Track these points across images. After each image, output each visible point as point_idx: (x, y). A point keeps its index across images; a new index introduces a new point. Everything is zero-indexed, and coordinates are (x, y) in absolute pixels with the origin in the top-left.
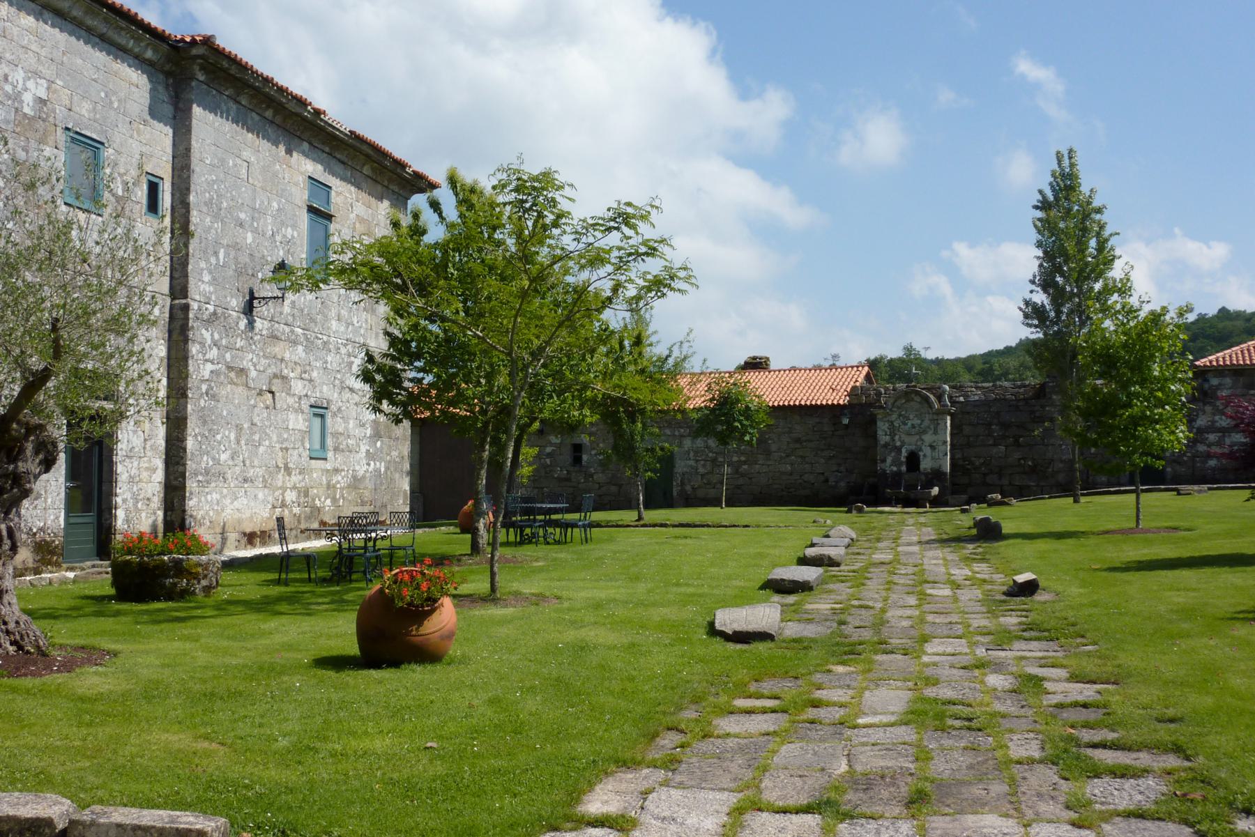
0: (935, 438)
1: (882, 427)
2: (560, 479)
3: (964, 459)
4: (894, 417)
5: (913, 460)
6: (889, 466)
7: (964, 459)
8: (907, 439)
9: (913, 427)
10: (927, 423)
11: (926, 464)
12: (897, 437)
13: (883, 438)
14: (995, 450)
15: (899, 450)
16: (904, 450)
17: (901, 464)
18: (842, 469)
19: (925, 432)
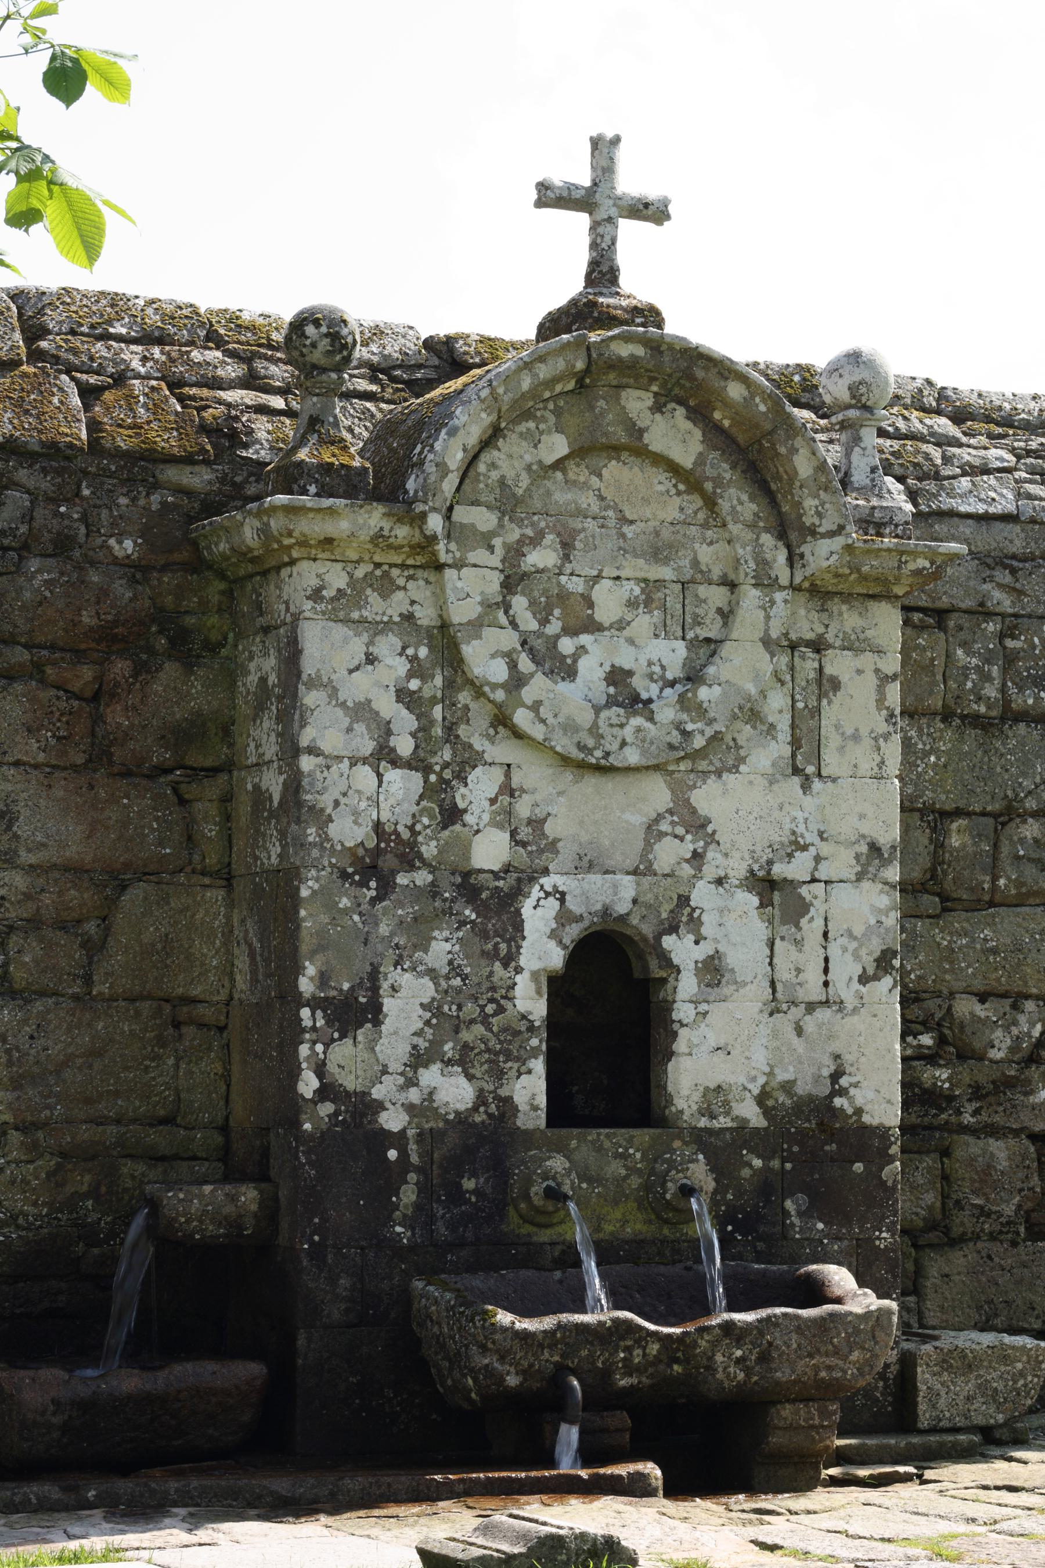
0: (801, 809)
1: (350, 674)
4: (470, 587)
6: (408, 1057)
8: (571, 811)
9: (623, 692)
10: (743, 666)
11: (721, 1056)
12: (478, 791)
13: (361, 798)
15: (491, 906)
16: (537, 916)
17: (496, 1060)
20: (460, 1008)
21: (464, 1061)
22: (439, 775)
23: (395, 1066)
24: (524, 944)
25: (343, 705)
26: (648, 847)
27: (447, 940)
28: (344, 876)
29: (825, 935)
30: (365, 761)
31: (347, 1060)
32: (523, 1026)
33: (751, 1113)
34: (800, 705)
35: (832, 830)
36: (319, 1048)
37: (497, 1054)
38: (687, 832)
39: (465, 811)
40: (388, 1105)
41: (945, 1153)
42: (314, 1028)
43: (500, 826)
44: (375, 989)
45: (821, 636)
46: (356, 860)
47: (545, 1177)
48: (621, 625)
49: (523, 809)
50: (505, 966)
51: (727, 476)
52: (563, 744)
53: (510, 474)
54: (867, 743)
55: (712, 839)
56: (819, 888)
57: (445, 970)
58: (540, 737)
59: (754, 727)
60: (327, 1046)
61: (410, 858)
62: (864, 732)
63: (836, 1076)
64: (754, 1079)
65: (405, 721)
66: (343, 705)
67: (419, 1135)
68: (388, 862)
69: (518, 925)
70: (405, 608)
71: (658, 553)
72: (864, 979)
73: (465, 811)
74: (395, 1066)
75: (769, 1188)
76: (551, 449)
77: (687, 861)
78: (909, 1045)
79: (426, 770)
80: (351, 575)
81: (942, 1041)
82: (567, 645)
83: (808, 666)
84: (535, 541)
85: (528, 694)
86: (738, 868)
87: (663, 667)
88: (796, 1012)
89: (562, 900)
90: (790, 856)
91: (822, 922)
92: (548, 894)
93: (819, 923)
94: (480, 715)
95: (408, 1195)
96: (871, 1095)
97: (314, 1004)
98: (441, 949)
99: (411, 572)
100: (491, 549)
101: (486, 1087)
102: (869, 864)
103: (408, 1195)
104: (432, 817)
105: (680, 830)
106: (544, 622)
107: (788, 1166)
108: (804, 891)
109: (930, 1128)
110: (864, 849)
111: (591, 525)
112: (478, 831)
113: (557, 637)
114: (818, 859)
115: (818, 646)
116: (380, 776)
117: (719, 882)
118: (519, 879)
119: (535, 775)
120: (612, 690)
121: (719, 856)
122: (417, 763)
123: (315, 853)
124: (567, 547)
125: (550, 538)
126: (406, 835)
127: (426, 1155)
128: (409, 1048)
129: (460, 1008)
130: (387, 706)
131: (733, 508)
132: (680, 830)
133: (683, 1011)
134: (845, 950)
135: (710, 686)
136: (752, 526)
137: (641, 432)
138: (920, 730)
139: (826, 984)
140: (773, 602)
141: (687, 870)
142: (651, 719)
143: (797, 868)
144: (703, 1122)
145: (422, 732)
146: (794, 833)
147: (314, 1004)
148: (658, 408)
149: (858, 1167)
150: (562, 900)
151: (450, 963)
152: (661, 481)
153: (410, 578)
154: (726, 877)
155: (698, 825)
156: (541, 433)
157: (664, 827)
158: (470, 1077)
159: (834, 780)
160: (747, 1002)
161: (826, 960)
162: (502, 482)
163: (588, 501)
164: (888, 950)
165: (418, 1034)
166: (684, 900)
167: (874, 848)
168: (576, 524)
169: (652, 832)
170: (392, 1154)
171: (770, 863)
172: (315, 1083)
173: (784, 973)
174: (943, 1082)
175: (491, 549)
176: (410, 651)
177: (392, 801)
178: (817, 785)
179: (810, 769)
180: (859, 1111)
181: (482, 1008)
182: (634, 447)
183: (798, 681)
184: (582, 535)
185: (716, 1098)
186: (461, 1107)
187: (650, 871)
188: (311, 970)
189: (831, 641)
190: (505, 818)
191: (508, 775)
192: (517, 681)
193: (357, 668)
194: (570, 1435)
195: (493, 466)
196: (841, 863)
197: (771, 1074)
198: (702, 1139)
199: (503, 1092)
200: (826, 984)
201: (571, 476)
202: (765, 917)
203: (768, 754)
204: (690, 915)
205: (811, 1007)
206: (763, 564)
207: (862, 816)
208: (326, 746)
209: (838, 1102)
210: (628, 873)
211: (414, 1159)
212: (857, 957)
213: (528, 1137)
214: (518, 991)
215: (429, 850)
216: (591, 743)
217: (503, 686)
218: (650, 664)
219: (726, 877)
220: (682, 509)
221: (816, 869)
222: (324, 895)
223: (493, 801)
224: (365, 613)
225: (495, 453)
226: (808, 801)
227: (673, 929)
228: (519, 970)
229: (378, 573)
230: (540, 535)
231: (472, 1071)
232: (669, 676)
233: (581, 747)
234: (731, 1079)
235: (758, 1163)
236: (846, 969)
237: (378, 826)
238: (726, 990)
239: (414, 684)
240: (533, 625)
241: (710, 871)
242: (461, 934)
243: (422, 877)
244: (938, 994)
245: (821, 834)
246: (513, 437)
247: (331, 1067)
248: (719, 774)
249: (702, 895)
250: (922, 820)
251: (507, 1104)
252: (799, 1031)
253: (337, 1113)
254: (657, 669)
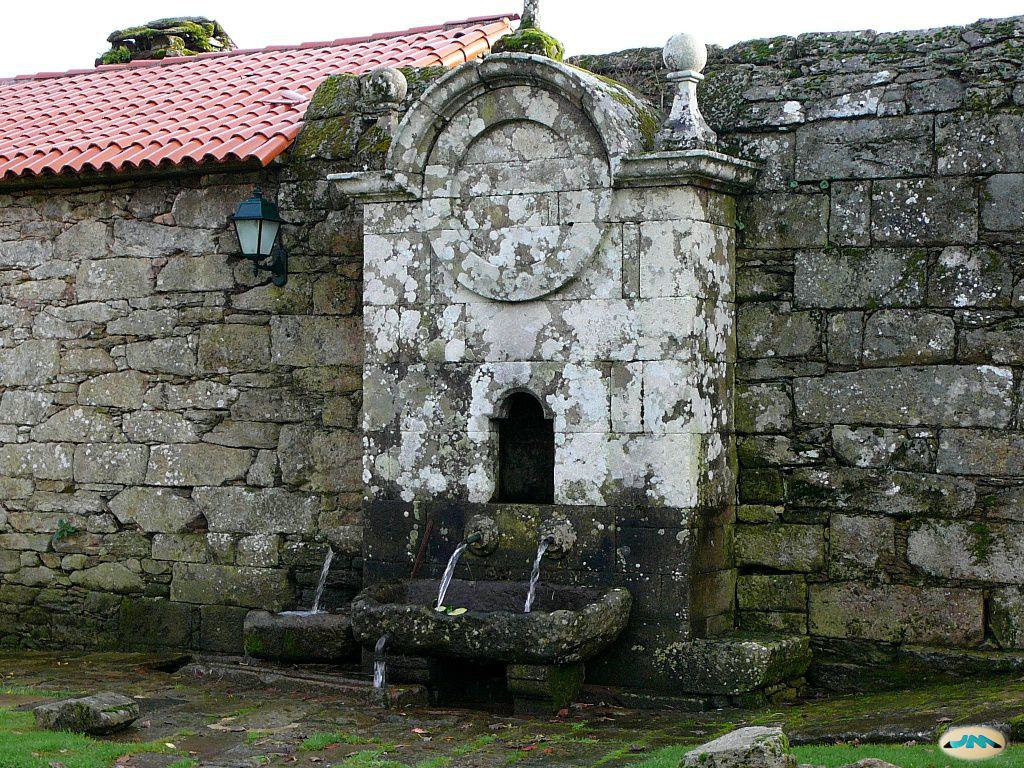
3: (798, 431)
4: (435, 209)
5: (525, 426)
7: (798, 431)
8: (492, 324)
9: (525, 261)
11: (582, 464)
12: (449, 318)
13: (389, 325)
15: (456, 382)
16: (479, 387)
17: (461, 462)
18: (261, 471)
20: (439, 437)
21: (441, 466)
22: (429, 312)
23: (408, 468)
24: (472, 402)
25: (382, 279)
26: (538, 345)
27: (433, 400)
28: (383, 368)
29: (642, 393)
30: (392, 307)
31: (386, 465)
32: (472, 446)
33: (596, 498)
34: (626, 256)
35: (647, 329)
36: (372, 457)
37: (458, 462)
38: (561, 336)
39: (442, 330)
40: (404, 488)
41: (827, 524)
42: (369, 447)
43: (460, 338)
44: (398, 427)
45: (640, 214)
46: (388, 359)
47: (476, 529)
48: (522, 221)
49: (471, 327)
50: (462, 414)
51: (573, 127)
52: (484, 291)
53: (454, 145)
54: (669, 275)
55: (575, 339)
56: (638, 365)
57: (432, 416)
58: (471, 288)
59: (599, 272)
60: (375, 456)
61: (415, 359)
62: (667, 270)
63: (648, 477)
64: (598, 478)
65: (412, 284)
66: (382, 279)
67: (419, 504)
68: (403, 359)
69: (469, 391)
70: (412, 224)
71: (543, 176)
72: (666, 419)
73: (442, 330)
74: (408, 468)
75: (606, 542)
76: (476, 128)
77: (560, 352)
78: (800, 456)
79: (422, 310)
80: (385, 210)
81: (824, 455)
82: (494, 235)
83: (631, 233)
84: (477, 179)
85: (465, 265)
86: (589, 355)
87: (547, 243)
88: (624, 439)
89: (492, 377)
90: (620, 346)
91: (640, 385)
92: (484, 374)
93: (638, 385)
94: (448, 281)
95: (414, 536)
96: (669, 489)
97: (369, 435)
98: (430, 405)
99: (415, 204)
100: (445, 187)
101: (452, 478)
102: (669, 349)
103: (414, 536)
104: (425, 335)
105: (557, 335)
106: (481, 223)
107: (619, 529)
108: (629, 367)
109: (816, 508)
110: (666, 340)
111: (506, 166)
112: (448, 341)
113: (489, 231)
114: (638, 347)
115: (638, 221)
116: (400, 314)
117: (579, 363)
118: (471, 363)
119: (477, 309)
120: (518, 258)
121: (579, 348)
122: (418, 306)
123: (370, 356)
124: (494, 179)
125: (485, 177)
126: (412, 345)
127: (424, 517)
128: (414, 458)
129: (439, 437)
130: (403, 276)
131: (576, 145)
132: (557, 335)
133: (559, 439)
134: (654, 401)
135: (564, 251)
136: (587, 155)
137: (524, 110)
138: (810, 259)
139: (642, 422)
140: (600, 198)
141: (560, 357)
142: (531, 274)
143: (624, 354)
144: (569, 502)
145: (420, 290)
146: (623, 333)
147: (369, 435)
148: (533, 95)
149: (662, 532)
150: (492, 377)
151: (434, 413)
152: (544, 136)
153: (413, 208)
154: (583, 360)
155: (566, 331)
156: (471, 120)
157: (547, 333)
158: (444, 474)
159: (648, 300)
160: (595, 433)
161: (643, 408)
162: (450, 150)
163: (505, 153)
164: (681, 401)
165: (419, 450)
166: (559, 375)
167: (673, 339)
168: (497, 166)
169: (541, 338)
170: (406, 514)
171: (609, 351)
172: (370, 476)
173: (617, 416)
174: (825, 480)
175: (445, 187)
176: (414, 247)
177: (405, 327)
178: (637, 303)
179: (633, 294)
180: (662, 498)
181: (451, 436)
182: (521, 121)
183: (625, 242)
184: (502, 172)
185: (577, 488)
186: (441, 490)
187: (540, 359)
188: (367, 418)
189: (645, 216)
190: (462, 333)
191: (463, 309)
192: (459, 257)
193: (389, 258)
194: (380, 669)
195: (446, 142)
196: (652, 349)
197: (608, 475)
198: (570, 511)
199: (461, 483)
200: (642, 422)
201: (495, 140)
202: (606, 383)
203: (607, 287)
204: (562, 383)
205: (633, 436)
206: (593, 175)
207: (665, 321)
208: (374, 301)
209: (649, 492)
210: (528, 361)
211: (417, 517)
212: (661, 405)
213: (476, 508)
214: (469, 428)
215: (424, 353)
216: (498, 289)
217: (452, 261)
218: (540, 240)
219: (583, 360)
220: (556, 150)
221: (636, 353)
222: (374, 379)
223: (456, 324)
224: (392, 229)
225: (447, 134)
226: (632, 314)
227: (553, 392)
228: (469, 416)
229: (399, 206)
230: (480, 175)
231: (445, 471)
232: (551, 247)
233: (493, 292)
234: (586, 477)
235: (601, 527)
236: (654, 413)
237: (399, 341)
238: (583, 425)
239: (416, 264)
240: (477, 226)
241: (574, 358)
242: (439, 397)
243: (421, 367)
244: (822, 425)
245: (639, 333)
246: (456, 124)
247: (377, 468)
248: (579, 300)
249: (569, 371)
250: (811, 316)
251: (463, 491)
252: (626, 449)
253: (380, 491)
254: (544, 243)
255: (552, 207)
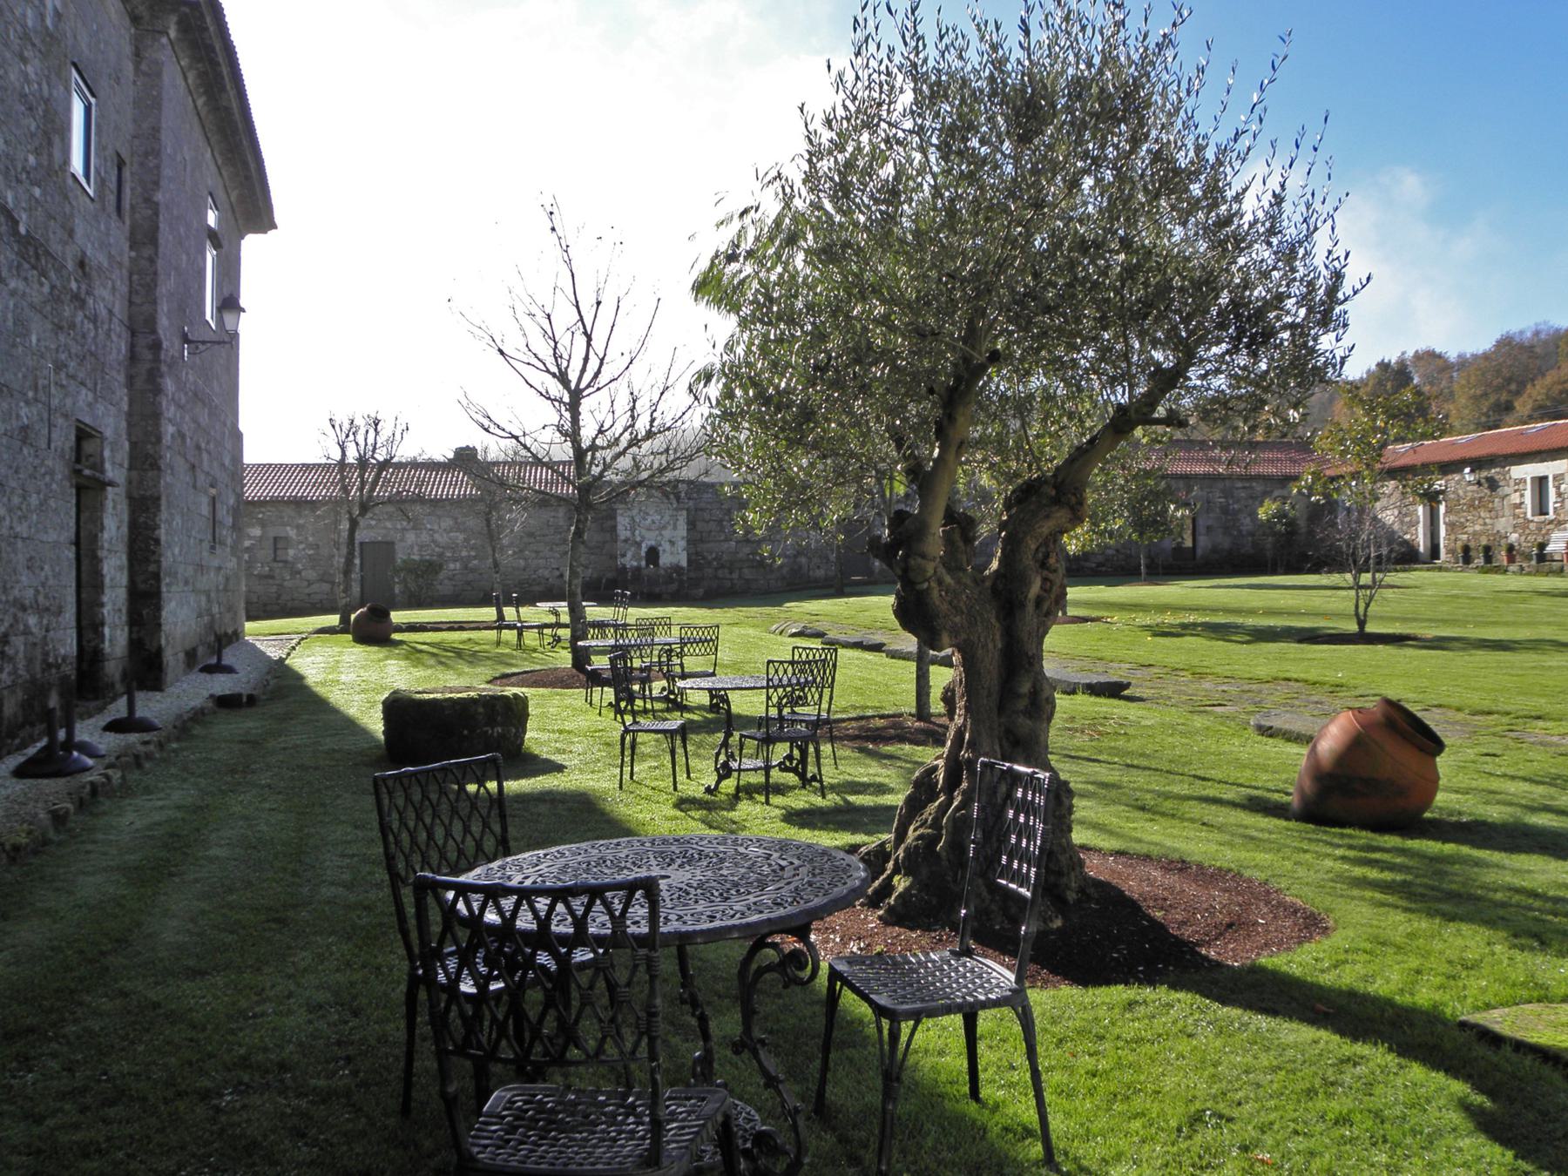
1: (622, 521)
2: (261, 577)
4: (635, 512)
5: (653, 554)
6: (629, 561)
8: (647, 534)
10: (667, 518)
11: (665, 560)
13: (623, 533)
14: (725, 546)
15: (639, 545)
19: (664, 527)
255: (659, 512)
